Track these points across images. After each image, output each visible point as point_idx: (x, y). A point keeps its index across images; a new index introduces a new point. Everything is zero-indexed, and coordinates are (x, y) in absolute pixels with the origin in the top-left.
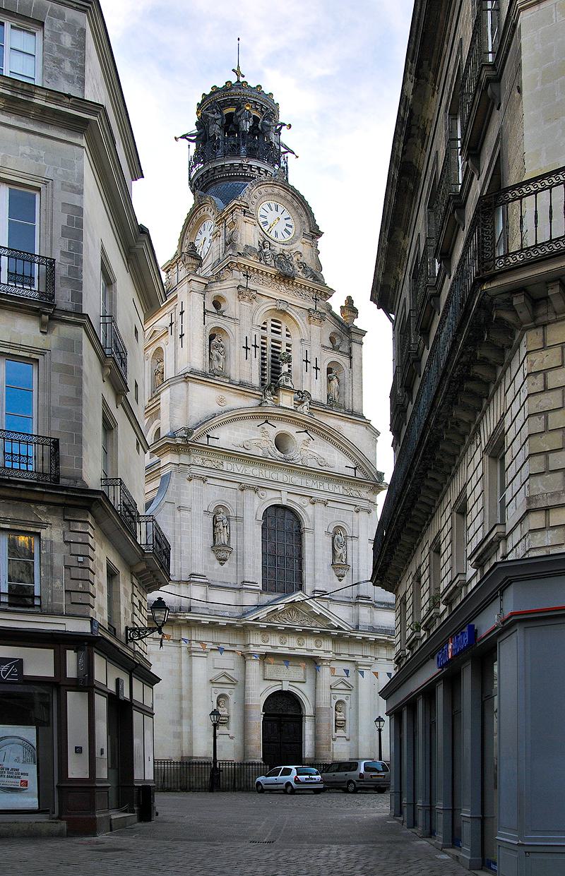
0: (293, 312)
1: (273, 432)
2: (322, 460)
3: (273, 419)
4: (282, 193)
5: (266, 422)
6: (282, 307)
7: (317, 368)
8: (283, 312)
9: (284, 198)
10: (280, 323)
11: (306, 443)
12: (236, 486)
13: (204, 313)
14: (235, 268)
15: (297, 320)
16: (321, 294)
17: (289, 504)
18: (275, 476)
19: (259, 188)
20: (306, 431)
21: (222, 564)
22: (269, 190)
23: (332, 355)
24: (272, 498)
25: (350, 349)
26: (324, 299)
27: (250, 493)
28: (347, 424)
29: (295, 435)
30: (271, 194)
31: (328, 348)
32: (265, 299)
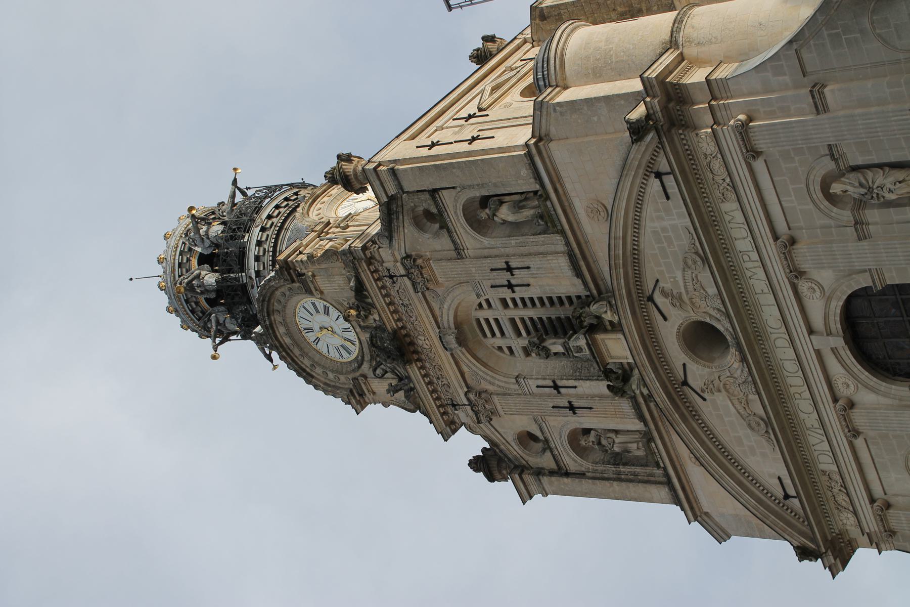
1: (698, 373)
2: (690, 262)
3: (670, 372)
4: (281, 330)
5: (685, 383)
6: (453, 344)
8: (461, 341)
9: (285, 324)
11: (677, 300)
12: (859, 442)
13: (567, 474)
16: (376, 271)
17: (836, 324)
18: (791, 366)
19: (308, 370)
20: (651, 299)
22: (297, 352)
23: (460, 231)
26: (376, 255)
27: (858, 418)
28: (572, 194)
30: (301, 349)
31: (454, 242)
32: (465, 369)
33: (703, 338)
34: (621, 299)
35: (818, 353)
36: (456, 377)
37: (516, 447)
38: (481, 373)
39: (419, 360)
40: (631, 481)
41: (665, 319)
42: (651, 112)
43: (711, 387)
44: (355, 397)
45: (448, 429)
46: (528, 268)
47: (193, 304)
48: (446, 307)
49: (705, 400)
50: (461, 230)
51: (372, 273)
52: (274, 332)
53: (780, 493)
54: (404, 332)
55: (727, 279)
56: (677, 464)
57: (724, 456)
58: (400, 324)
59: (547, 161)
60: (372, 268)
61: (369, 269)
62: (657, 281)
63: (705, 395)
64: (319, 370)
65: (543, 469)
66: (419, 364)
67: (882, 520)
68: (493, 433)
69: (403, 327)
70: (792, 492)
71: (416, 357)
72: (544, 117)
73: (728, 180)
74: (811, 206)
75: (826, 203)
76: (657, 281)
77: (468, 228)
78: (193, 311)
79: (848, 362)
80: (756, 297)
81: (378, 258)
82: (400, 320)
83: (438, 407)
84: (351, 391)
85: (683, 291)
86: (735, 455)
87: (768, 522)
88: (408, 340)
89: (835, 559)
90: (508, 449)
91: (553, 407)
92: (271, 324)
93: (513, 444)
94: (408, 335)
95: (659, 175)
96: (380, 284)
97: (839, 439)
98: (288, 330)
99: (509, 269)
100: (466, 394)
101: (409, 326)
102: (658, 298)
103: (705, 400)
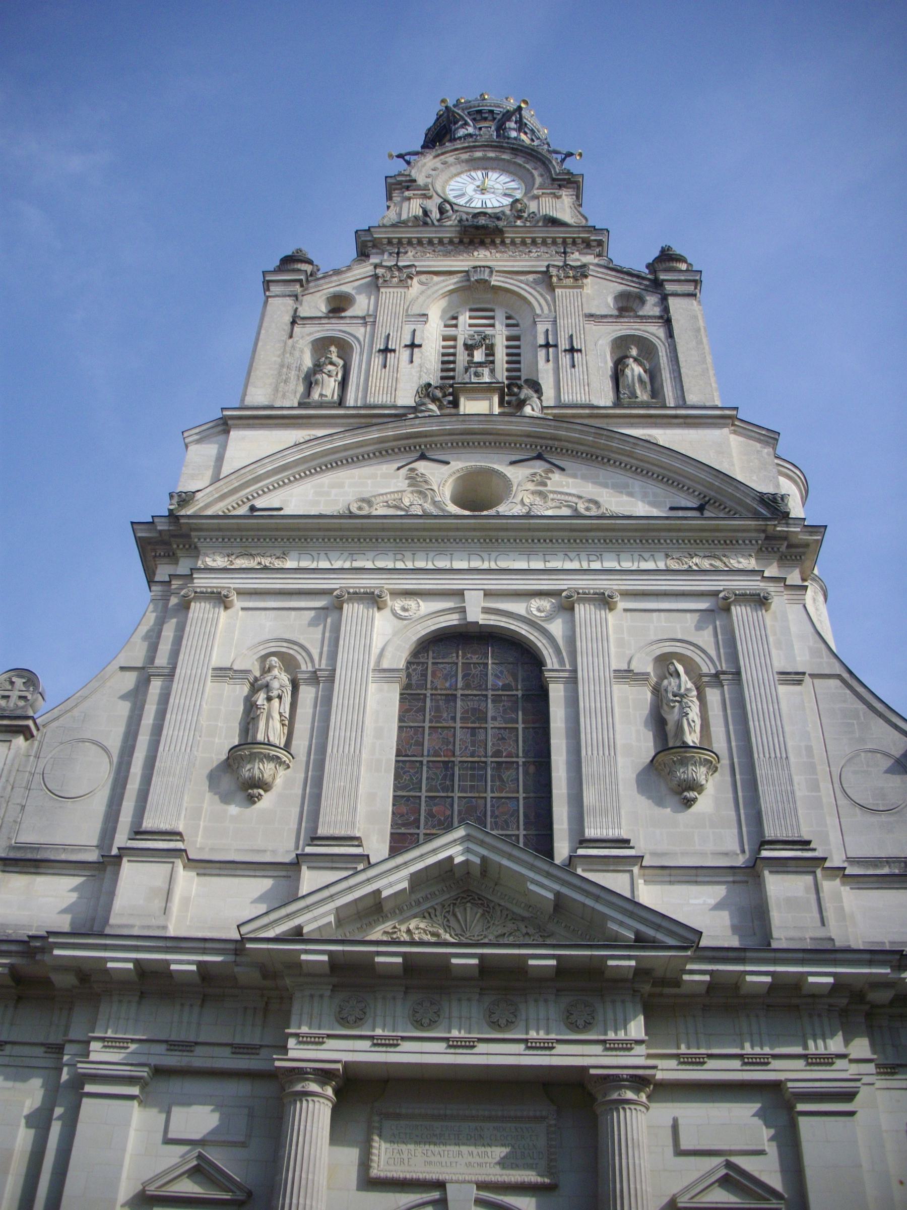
0: (511, 281)
3: (442, 446)
4: (491, 154)
5: (423, 457)
7: (572, 350)
10: (492, 310)
13: (293, 323)
14: (374, 251)
15: (522, 292)
16: (574, 243)
19: (442, 157)
20: (539, 457)
21: (252, 800)
22: (465, 156)
23: (618, 327)
24: (429, 615)
25: (666, 310)
26: (589, 251)
29: (512, 473)
31: (605, 316)
33: (477, 494)
34: (555, 426)
35: (460, 594)
36: (434, 266)
37: (332, 290)
38: (436, 288)
39: (461, 242)
40: (280, 374)
41: (513, 463)
42: (791, 521)
43: (416, 482)
44: (406, 181)
45: (369, 239)
46: (574, 366)
47: (486, 115)
48: (523, 286)
49: (399, 469)
50: (618, 328)
51: (574, 239)
52: (492, 146)
53: (259, 503)
54: (498, 241)
55: (572, 530)
56: (305, 421)
57: (322, 464)
58: (508, 241)
59: (710, 421)
60: (579, 241)
61: (579, 238)
62: (563, 470)
63: (404, 471)
64: (439, 165)
65: (301, 304)
66: (456, 240)
67: (212, 593)
68: (354, 275)
69: (503, 242)
70: (255, 514)
71: (466, 240)
72: (757, 436)
73: (695, 568)
74: (653, 638)
75: (658, 652)
76: (563, 470)
77: (619, 334)
78: (480, 112)
79: (441, 619)
80: (541, 554)
81: (585, 251)
82: (513, 243)
83: (400, 239)
84: (415, 181)
85: (549, 488)
86: (317, 477)
87: (233, 477)
88: (488, 241)
89: (160, 532)
90: (331, 282)
91: (389, 335)
92: (502, 147)
93: (337, 289)
94: (493, 243)
95: (701, 509)
96: (559, 241)
97: (334, 581)
98: (491, 159)
99: (572, 350)
100: (416, 267)
101: (502, 248)
102: (539, 467)
103: (399, 469)
